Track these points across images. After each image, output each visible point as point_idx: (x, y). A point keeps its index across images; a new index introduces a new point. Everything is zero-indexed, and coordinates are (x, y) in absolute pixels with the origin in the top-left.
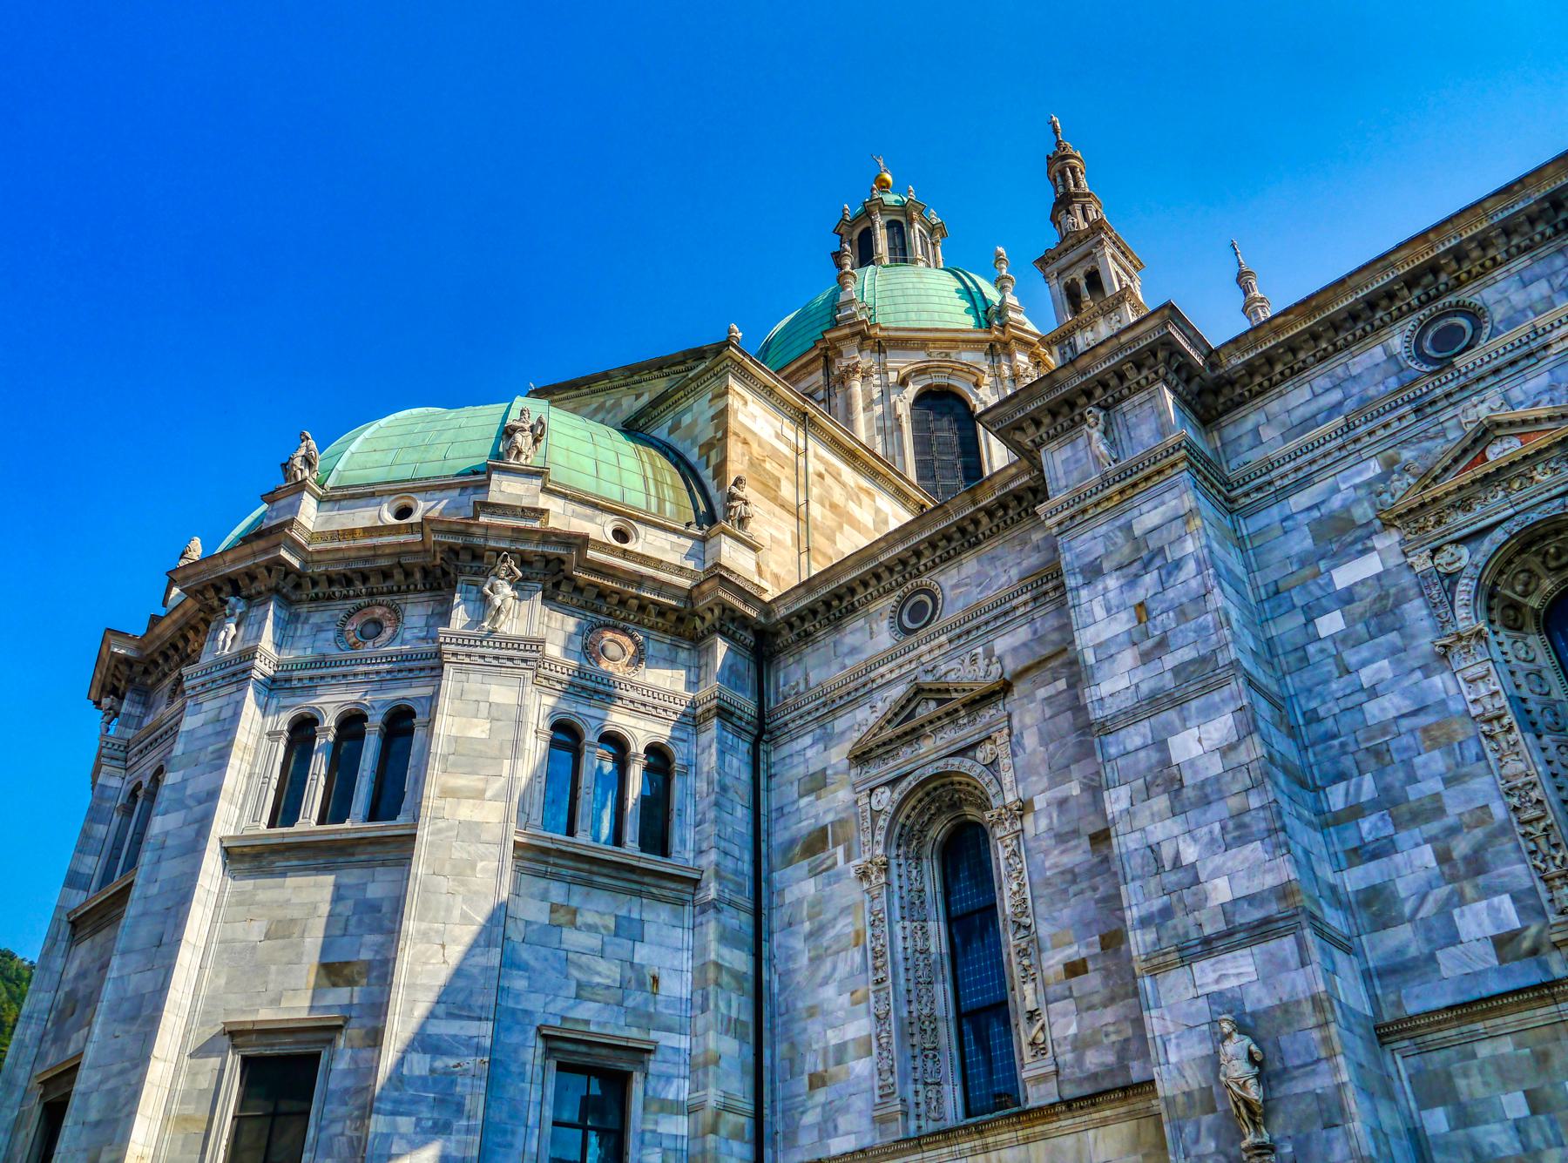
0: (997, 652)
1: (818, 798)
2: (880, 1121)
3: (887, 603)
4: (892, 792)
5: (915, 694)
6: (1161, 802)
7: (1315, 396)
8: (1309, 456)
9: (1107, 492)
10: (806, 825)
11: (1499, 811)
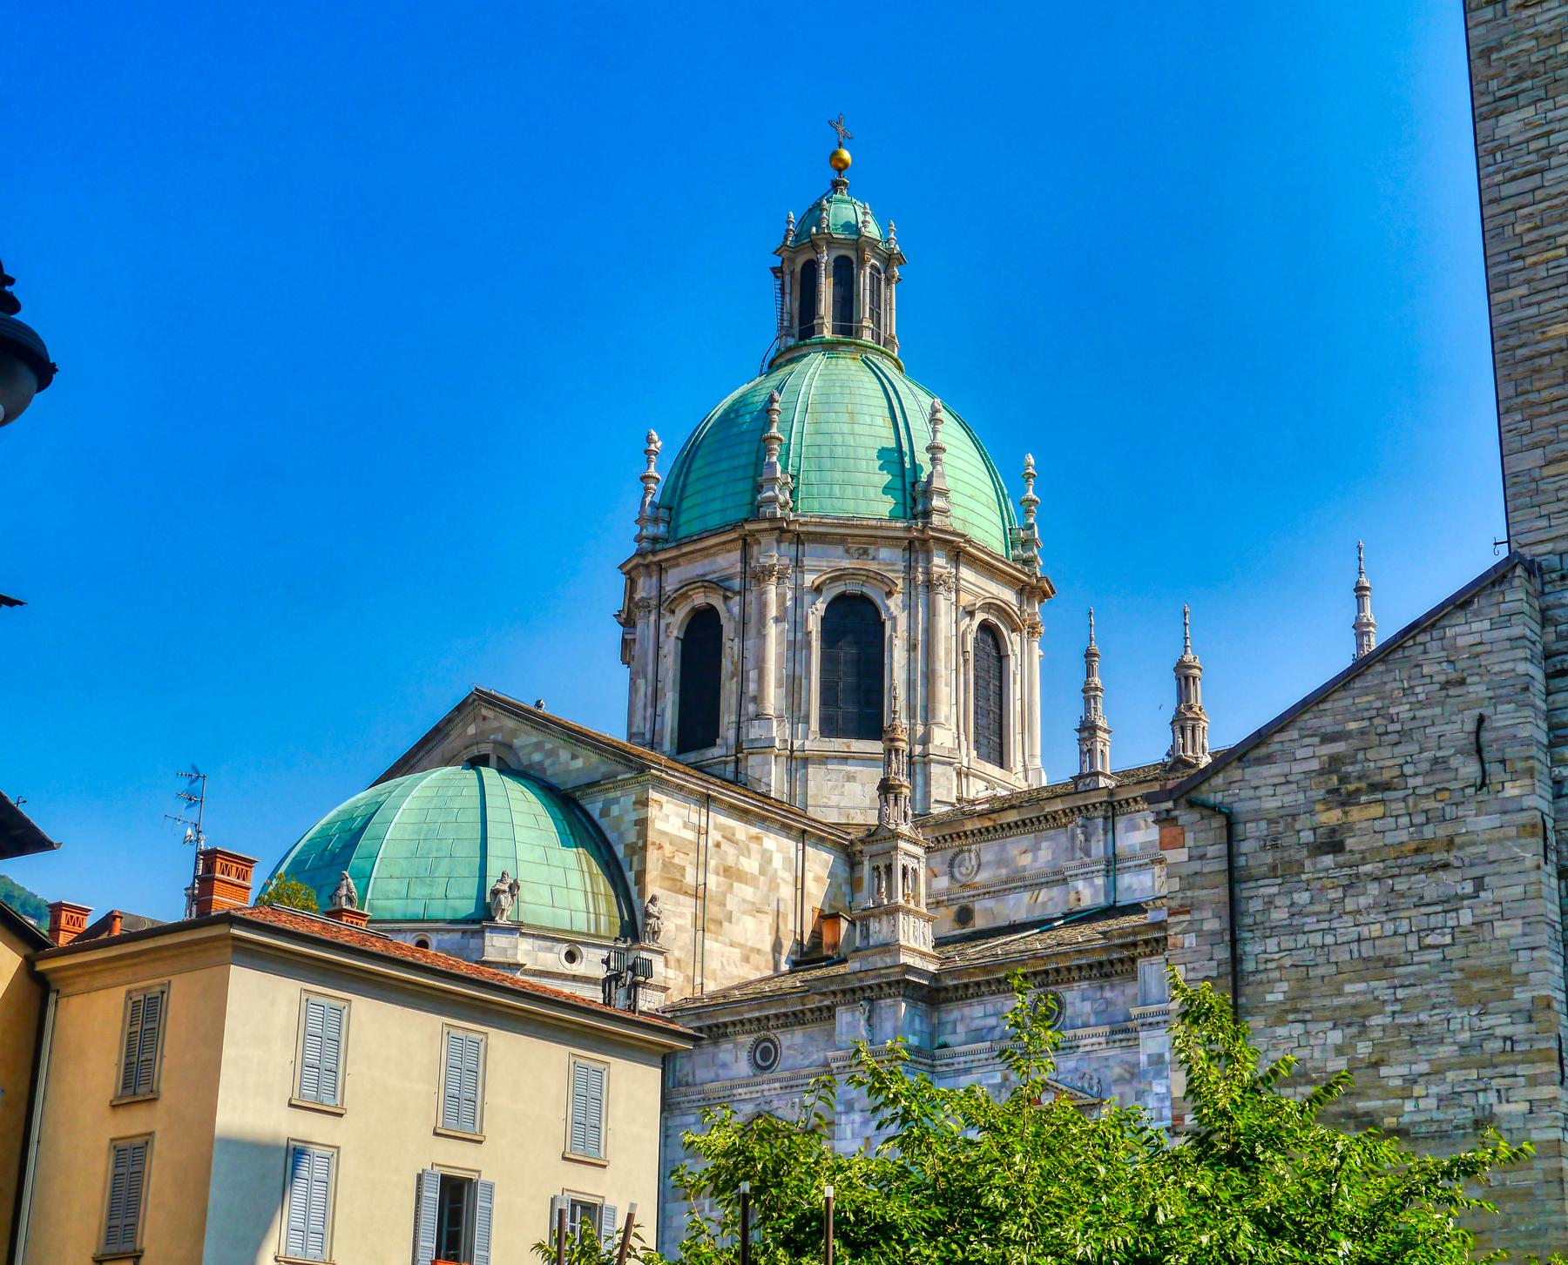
3: (747, 1040)
8: (972, 1058)
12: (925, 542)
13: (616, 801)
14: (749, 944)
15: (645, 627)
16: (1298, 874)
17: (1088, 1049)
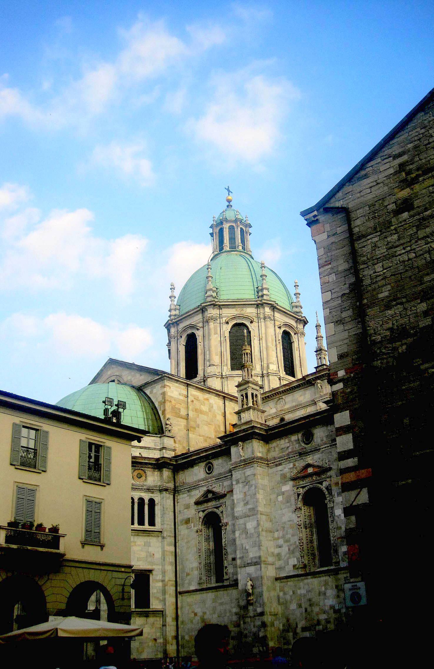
2: (200, 584)
4: (203, 513)
6: (244, 536)
8: (281, 459)
9: (242, 464)
10: (186, 517)
11: (297, 543)
14: (206, 435)
15: (173, 344)
16: (389, 227)
17: (323, 450)
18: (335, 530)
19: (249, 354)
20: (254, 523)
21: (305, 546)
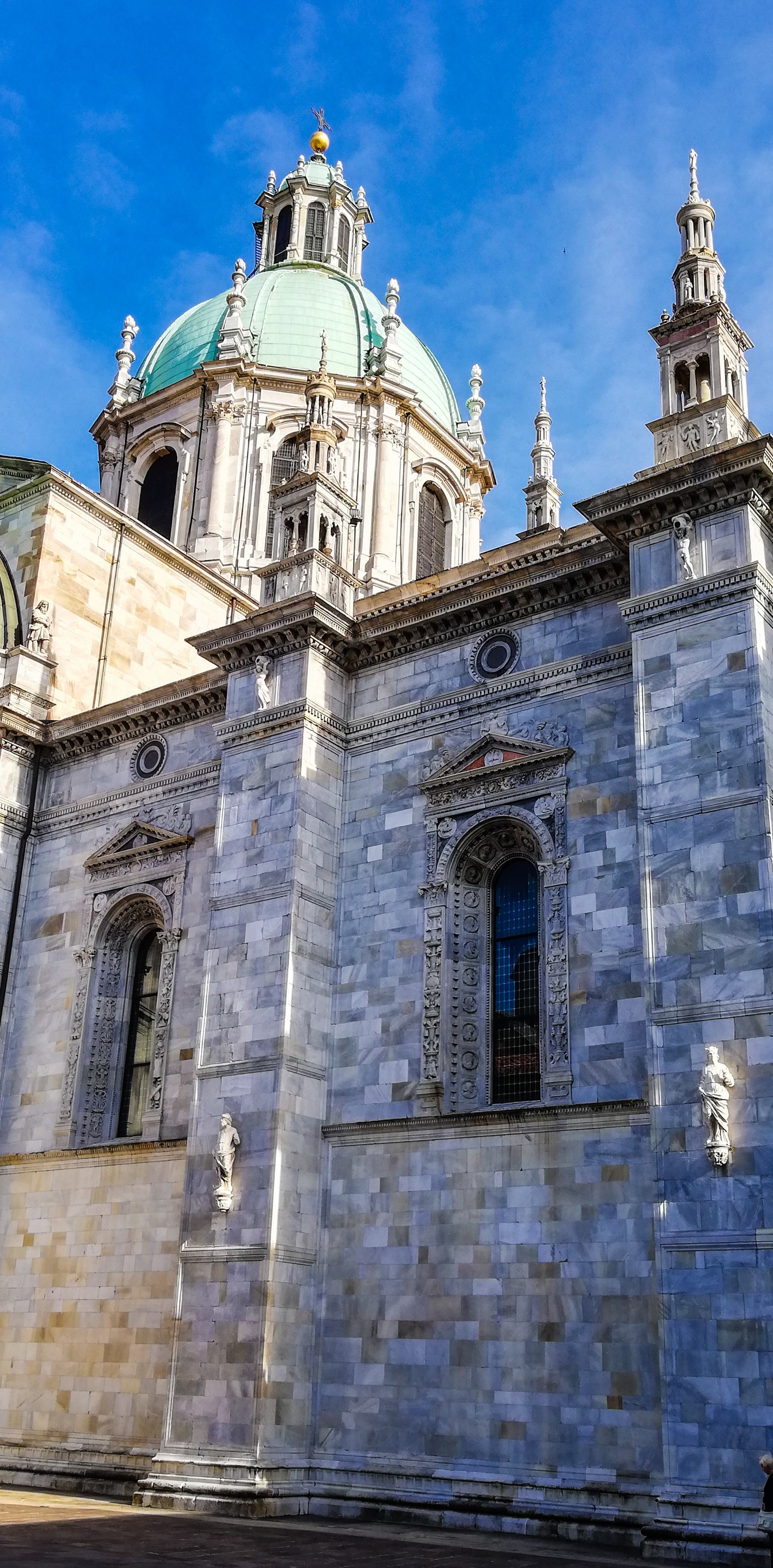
0: (191, 811)
1: (62, 891)
3: (131, 746)
5: (135, 829)
7: (415, 674)
8: (395, 724)
10: (50, 911)
11: (418, 1008)
12: (376, 396)
13: (15, 516)
17: (550, 691)
18: (566, 966)
19: (329, 401)
20: (274, 925)
21: (444, 1017)
